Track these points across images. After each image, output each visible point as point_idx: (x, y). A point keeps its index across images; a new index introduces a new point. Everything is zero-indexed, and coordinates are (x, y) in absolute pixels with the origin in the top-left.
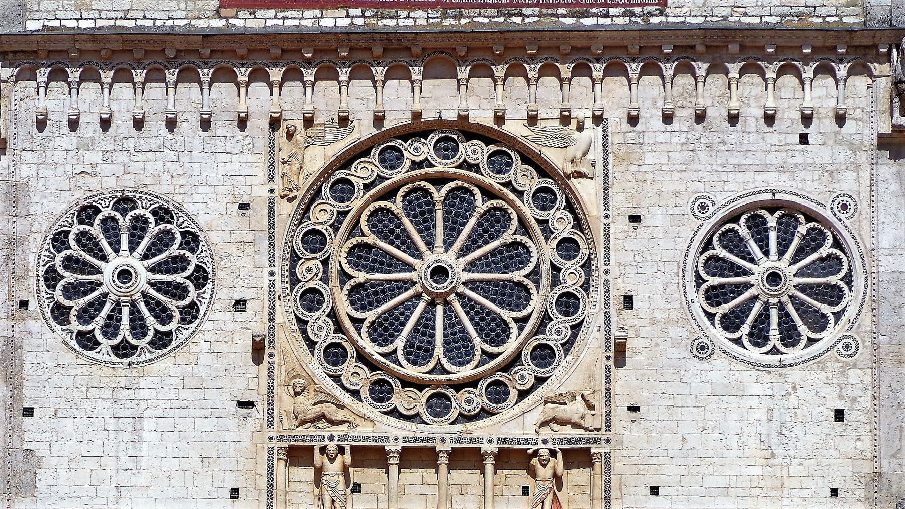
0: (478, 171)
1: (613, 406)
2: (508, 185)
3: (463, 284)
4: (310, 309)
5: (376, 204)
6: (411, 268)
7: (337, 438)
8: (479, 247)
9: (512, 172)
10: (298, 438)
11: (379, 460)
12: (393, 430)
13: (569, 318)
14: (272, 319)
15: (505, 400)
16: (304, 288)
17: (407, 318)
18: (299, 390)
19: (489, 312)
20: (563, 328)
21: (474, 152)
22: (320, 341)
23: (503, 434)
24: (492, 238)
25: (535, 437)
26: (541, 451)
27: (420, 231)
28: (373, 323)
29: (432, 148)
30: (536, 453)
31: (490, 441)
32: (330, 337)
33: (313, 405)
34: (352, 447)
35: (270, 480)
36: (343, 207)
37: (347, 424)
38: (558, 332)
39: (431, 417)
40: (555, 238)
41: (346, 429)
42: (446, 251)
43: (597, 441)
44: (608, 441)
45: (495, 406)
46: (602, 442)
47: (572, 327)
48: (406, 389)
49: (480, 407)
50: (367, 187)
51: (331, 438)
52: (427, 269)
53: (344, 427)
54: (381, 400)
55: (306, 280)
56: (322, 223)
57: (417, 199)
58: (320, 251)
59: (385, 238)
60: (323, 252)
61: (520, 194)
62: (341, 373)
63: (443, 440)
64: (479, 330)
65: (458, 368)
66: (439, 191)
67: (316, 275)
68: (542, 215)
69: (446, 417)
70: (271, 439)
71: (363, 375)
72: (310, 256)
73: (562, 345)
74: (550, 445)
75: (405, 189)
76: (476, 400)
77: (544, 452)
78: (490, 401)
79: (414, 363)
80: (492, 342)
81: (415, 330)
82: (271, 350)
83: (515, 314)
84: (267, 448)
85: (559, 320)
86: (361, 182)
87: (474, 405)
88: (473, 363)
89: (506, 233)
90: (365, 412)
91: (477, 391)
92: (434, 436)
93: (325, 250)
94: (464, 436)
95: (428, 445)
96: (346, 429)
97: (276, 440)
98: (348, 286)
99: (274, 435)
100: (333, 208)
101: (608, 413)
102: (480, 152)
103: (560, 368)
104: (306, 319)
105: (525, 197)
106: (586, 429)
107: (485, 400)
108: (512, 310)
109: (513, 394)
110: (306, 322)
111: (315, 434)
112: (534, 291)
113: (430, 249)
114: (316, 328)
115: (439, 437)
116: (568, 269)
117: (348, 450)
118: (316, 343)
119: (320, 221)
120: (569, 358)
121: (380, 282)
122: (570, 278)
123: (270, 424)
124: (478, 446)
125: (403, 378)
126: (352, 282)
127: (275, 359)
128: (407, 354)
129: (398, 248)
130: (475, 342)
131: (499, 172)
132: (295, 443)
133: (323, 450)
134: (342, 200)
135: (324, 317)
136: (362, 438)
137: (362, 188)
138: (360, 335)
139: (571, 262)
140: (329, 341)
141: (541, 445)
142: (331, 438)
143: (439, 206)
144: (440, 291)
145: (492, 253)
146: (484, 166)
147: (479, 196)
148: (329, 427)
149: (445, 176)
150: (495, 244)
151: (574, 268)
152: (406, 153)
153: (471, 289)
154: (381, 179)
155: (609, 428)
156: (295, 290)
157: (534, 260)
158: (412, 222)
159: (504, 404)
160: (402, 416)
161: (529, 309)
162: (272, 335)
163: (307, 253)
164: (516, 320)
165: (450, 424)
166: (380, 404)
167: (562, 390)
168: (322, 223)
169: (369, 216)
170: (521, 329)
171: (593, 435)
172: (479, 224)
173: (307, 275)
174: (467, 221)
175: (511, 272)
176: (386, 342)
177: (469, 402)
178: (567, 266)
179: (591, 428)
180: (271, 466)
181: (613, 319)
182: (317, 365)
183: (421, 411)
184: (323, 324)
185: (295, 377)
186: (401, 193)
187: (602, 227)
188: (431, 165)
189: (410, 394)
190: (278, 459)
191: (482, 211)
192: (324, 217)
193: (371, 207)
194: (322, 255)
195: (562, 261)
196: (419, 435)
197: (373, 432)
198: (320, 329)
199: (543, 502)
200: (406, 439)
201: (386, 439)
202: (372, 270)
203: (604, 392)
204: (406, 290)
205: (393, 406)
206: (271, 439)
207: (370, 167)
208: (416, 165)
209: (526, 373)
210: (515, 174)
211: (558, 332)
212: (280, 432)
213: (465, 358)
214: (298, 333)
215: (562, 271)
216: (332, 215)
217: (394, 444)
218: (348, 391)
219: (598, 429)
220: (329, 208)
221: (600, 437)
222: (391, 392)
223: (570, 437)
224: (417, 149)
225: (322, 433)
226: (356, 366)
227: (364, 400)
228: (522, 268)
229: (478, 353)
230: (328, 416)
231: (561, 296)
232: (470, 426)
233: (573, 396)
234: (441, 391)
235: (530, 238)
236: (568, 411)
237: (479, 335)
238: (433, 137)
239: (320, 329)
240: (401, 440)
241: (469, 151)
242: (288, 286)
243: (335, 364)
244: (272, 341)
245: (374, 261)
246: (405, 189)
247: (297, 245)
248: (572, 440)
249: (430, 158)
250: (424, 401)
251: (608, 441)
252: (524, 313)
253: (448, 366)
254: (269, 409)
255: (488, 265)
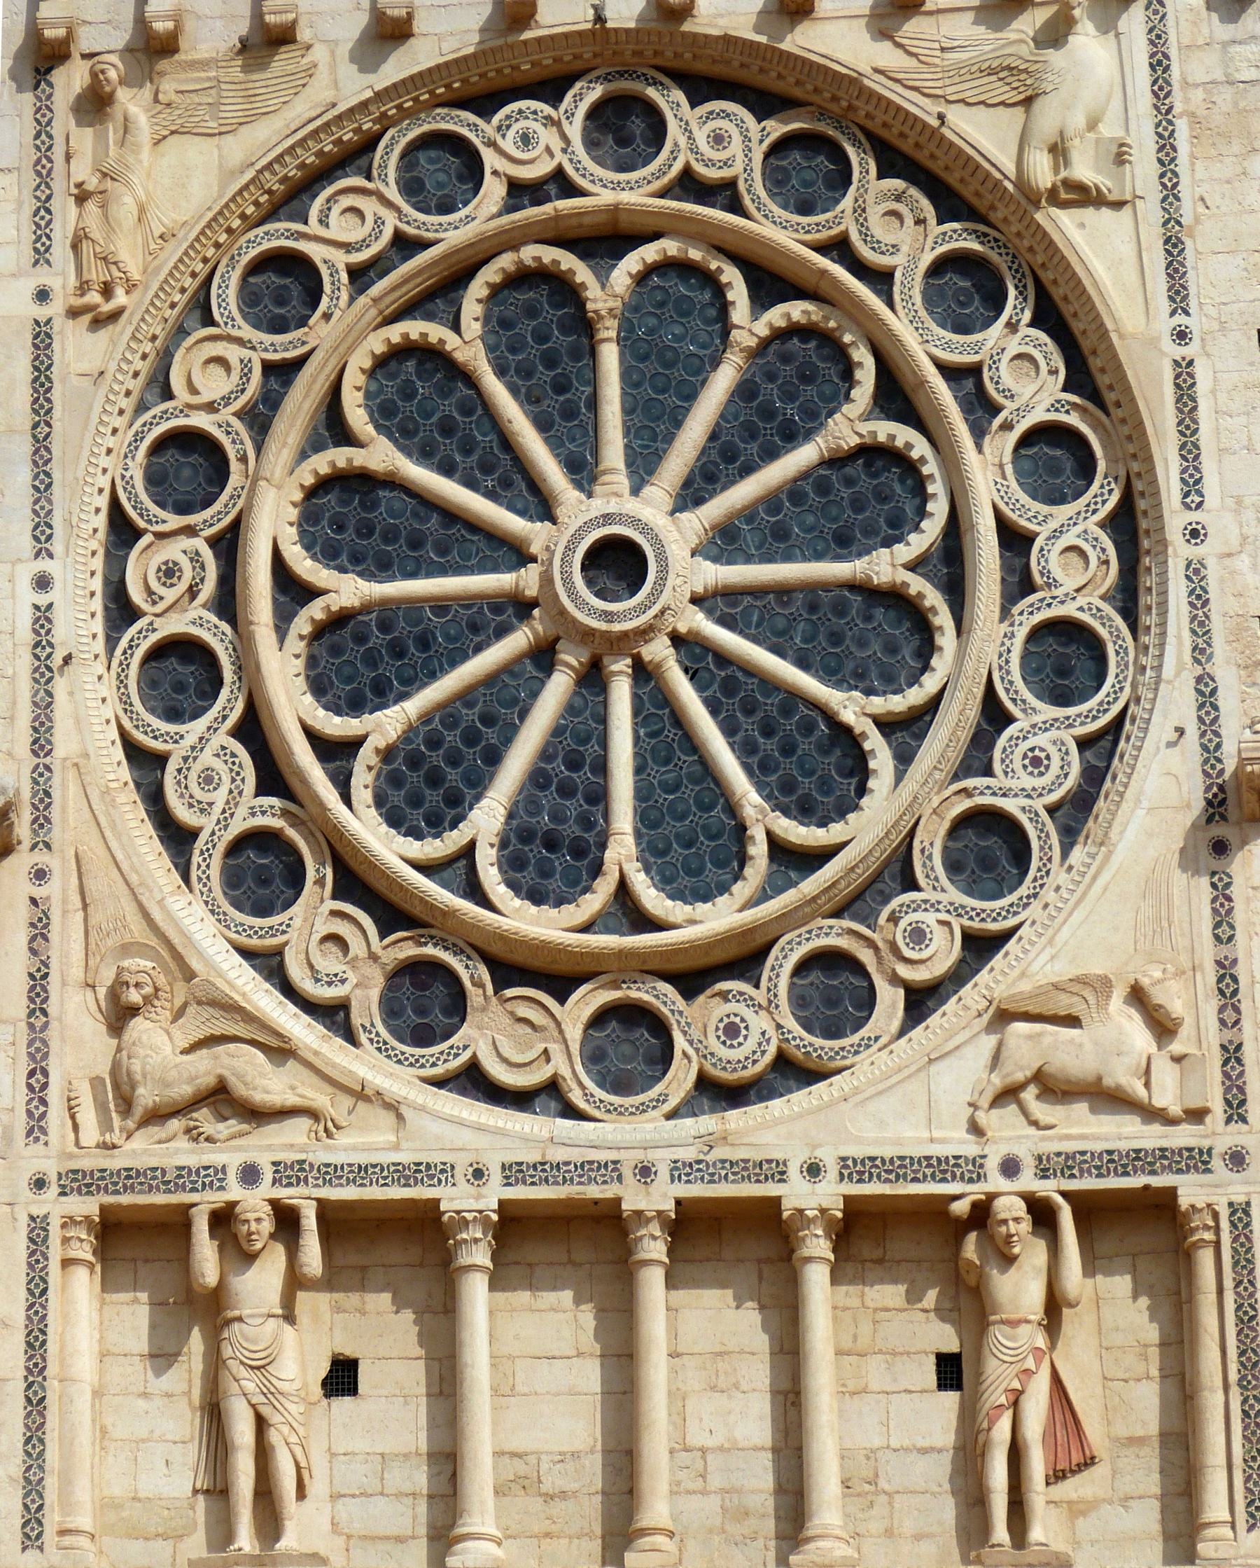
0: (736, 207)
1: (1246, 1024)
2: (839, 248)
3: (696, 600)
4: (174, 714)
5: (395, 333)
6: (518, 555)
7: (268, 1176)
8: (747, 470)
9: (847, 203)
10: (131, 1178)
11: (421, 1265)
12: (467, 1137)
13: (1072, 711)
14: (41, 744)
15: (859, 1025)
16: (154, 638)
17: (509, 734)
18: (134, 997)
19: (793, 698)
20: (1053, 750)
21: (718, 139)
22: (207, 824)
23: (858, 1141)
24: (792, 436)
25: (970, 1148)
26: (999, 1203)
27: (543, 425)
28: (387, 754)
29: (575, 130)
30: (982, 1213)
31: (814, 1170)
32: (242, 811)
33: (185, 1052)
34: (325, 1210)
35: (36, 1342)
36: (281, 346)
37: (304, 1123)
38: (1036, 762)
39: (600, 1094)
40: (1007, 426)
41: (302, 1139)
42: (635, 491)
43: (1198, 1160)
44: (1237, 1159)
45: (828, 1044)
46: (1217, 1163)
47: (1084, 743)
48: (510, 992)
49: (772, 1050)
50: (360, 276)
51: (250, 1175)
52: (570, 549)
53: (296, 1132)
54: (423, 1036)
55: (159, 608)
56: (211, 407)
57: (531, 311)
58: (207, 503)
59: (425, 455)
60: (217, 506)
61: (881, 279)
62: (280, 939)
63: (645, 1172)
64: (759, 770)
65: (688, 908)
66: (603, 278)
67: (192, 592)
68: (959, 349)
69: (654, 1092)
70: (39, 1184)
71: (357, 946)
72: (174, 521)
73: (1052, 810)
74: (1028, 1181)
75: (490, 274)
76: (759, 1023)
77: (1010, 1208)
78: (808, 1028)
79: (537, 897)
80: (805, 811)
81: (537, 778)
82: (41, 858)
83: (878, 704)
84: (24, 1220)
85: (1038, 719)
86: (341, 259)
87: (750, 1045)
88: (743, 890)
89: (837, 416)
90: (363, 1072)
91: (760, 996)
92: (613, 1155)
93: (224, 497)
94: (719, 1153)
95: (594, 1192)
96: (302, 1139)
97: (54, 1190)
98: (302, 624)
99: (51, 1168)
100: (246, 353)
101: (1232, 1054)
102: (737, 138)
103: (1048, 895)
104: (158, 745)
105: (896, 289)
106: (1152, 1114)
107: (791, 1023)
108: (869, 692)
109: (890, 1001)
110: (160, 760)
111: (192, 1161)
112: (943, 618)
113: (579, 485)
114: (193, 776)
115: (629, 1159)
116: (1056, 534)
117: (310, 1221)
118: (193, 834)
119: (205, 397)
120: (1078, 854)
121: (412, 606)
122: (1065, 567)
123: (36, 1129)
124: (770, 1190)
125: (496, 949)
126: (316, 610)
127: (51, 890)
128: (512, 865)
129: (471, 484)
130: (749, 813)
131: (805, 208)
132: (126, 1199)
133: (223, 1220)
134: (278, 326)
135: (222, 738)
136: (362, 1173)
137: (344, 277)
138: (347, 799)
139: (1064, 511)
140: (238, 826)
141: (995, 1182)
142: (250, 1175)
143: (608, 330)
144: (617, 627)
145: (794, 491)
146: (755, 189)
147: (738, 293)
148: (241, 1135)
149: (625, 223)
150: (804, 456)
151: (1079, 529)
152: (490, 159)
153: (726, 622)
154: (405, 245)
155: (1236, 1110)
156: (124, 643)
157: (939, 508)
158: (514, 391)
159: (855, 1038)
160: (497, 1094)
161: (930, 684)
162: (43, 798)
163: (162, 514)
164: (886, 725)
165: (670, 1116)
166: (418, 1051)
167: (1062, 970)
168: (211, 407)
169: (371, 374)
170: (904, 759)
171: (1183, 1136)
172: (744, 391)
173: (161, 591)
174: (704, 383)
175: (860, 555)
176: (437, 824)
177: (732, 1031)
178: (1053, 525)
179: (1175, 1110)
180: (38, 1290)
181: (1227, 701)
182: (199, 909)
183: (565, 1072)
184: (218, 764)
185: (126, 949)
186: (477, 289)
187: (1168, 374)
188: (571, 190)
189: (524, 1011)
190: (67, 1263)
191: (752, 342)
192: (214, 385)
193: (377, 343)
194: (213, 518)
195: (1037, 506)
196: (558, 1155)
197: (396, 1147)
198: (208, 779)
199: (1016, 1404)
200: (514, 1172)
201: (443, 1173)
202: (382, 568)
203: (1210, 975)
204: (502, 631)
205: (465, 1056)
206: (39, 1184)
207: (369, 206)
208: (519, 192)
209: (930, 918)
210: (860, 211)
211: (1036, 762)
212: (71, 1156)
213: (712, 873)
214: (132, 794)
215: (1039, 542)
216: (246, 375)
217: (472, 1190)
218: (309, 1006)
219: (1197, 1115)
220: (233, 353)
221: (1205, 1144)
222: (457, 1006)
223: (1099, 1147)
224: (526, 140)
225: (215, 1157)
226: (335, 913)
227: (363, 1038)
228: (899, 539)
229: (759, 849)
230: (240, 1090)
231: (1037, 633)
232: (735, 1118)
233: (1103, 986)
234: (634, 994)
235: (920, 426)
236: (1088, 1046)
237: (760, 786)
238: (579, 97)
239: (208, 780)
240: (496, 1177)
241: (701, 137)
242: (98, 626)
243: (263, 910)
244: (41, 821)
245: (390, 535)
246: (490, 274)
247: (129, 482)
248: (1112, 1161)
249: (569, 169)
250: (575, 1033)
251: (1237, 1159)
252: (914, 696)
253: (651, 897)
254: (31, 1074)
255: (780, 533)
